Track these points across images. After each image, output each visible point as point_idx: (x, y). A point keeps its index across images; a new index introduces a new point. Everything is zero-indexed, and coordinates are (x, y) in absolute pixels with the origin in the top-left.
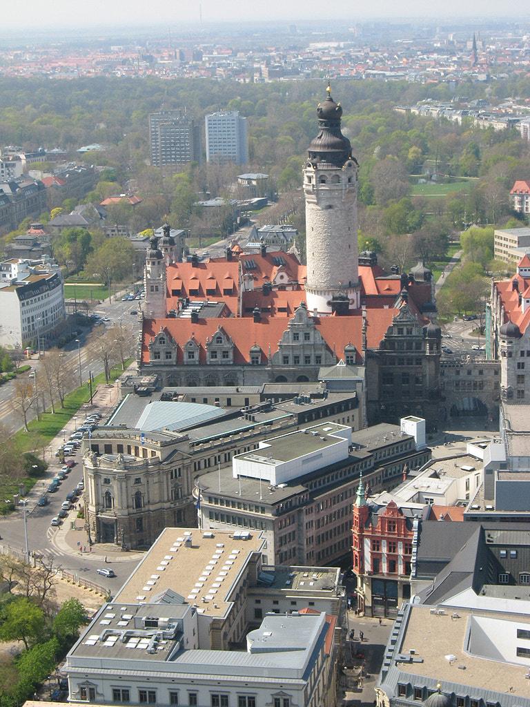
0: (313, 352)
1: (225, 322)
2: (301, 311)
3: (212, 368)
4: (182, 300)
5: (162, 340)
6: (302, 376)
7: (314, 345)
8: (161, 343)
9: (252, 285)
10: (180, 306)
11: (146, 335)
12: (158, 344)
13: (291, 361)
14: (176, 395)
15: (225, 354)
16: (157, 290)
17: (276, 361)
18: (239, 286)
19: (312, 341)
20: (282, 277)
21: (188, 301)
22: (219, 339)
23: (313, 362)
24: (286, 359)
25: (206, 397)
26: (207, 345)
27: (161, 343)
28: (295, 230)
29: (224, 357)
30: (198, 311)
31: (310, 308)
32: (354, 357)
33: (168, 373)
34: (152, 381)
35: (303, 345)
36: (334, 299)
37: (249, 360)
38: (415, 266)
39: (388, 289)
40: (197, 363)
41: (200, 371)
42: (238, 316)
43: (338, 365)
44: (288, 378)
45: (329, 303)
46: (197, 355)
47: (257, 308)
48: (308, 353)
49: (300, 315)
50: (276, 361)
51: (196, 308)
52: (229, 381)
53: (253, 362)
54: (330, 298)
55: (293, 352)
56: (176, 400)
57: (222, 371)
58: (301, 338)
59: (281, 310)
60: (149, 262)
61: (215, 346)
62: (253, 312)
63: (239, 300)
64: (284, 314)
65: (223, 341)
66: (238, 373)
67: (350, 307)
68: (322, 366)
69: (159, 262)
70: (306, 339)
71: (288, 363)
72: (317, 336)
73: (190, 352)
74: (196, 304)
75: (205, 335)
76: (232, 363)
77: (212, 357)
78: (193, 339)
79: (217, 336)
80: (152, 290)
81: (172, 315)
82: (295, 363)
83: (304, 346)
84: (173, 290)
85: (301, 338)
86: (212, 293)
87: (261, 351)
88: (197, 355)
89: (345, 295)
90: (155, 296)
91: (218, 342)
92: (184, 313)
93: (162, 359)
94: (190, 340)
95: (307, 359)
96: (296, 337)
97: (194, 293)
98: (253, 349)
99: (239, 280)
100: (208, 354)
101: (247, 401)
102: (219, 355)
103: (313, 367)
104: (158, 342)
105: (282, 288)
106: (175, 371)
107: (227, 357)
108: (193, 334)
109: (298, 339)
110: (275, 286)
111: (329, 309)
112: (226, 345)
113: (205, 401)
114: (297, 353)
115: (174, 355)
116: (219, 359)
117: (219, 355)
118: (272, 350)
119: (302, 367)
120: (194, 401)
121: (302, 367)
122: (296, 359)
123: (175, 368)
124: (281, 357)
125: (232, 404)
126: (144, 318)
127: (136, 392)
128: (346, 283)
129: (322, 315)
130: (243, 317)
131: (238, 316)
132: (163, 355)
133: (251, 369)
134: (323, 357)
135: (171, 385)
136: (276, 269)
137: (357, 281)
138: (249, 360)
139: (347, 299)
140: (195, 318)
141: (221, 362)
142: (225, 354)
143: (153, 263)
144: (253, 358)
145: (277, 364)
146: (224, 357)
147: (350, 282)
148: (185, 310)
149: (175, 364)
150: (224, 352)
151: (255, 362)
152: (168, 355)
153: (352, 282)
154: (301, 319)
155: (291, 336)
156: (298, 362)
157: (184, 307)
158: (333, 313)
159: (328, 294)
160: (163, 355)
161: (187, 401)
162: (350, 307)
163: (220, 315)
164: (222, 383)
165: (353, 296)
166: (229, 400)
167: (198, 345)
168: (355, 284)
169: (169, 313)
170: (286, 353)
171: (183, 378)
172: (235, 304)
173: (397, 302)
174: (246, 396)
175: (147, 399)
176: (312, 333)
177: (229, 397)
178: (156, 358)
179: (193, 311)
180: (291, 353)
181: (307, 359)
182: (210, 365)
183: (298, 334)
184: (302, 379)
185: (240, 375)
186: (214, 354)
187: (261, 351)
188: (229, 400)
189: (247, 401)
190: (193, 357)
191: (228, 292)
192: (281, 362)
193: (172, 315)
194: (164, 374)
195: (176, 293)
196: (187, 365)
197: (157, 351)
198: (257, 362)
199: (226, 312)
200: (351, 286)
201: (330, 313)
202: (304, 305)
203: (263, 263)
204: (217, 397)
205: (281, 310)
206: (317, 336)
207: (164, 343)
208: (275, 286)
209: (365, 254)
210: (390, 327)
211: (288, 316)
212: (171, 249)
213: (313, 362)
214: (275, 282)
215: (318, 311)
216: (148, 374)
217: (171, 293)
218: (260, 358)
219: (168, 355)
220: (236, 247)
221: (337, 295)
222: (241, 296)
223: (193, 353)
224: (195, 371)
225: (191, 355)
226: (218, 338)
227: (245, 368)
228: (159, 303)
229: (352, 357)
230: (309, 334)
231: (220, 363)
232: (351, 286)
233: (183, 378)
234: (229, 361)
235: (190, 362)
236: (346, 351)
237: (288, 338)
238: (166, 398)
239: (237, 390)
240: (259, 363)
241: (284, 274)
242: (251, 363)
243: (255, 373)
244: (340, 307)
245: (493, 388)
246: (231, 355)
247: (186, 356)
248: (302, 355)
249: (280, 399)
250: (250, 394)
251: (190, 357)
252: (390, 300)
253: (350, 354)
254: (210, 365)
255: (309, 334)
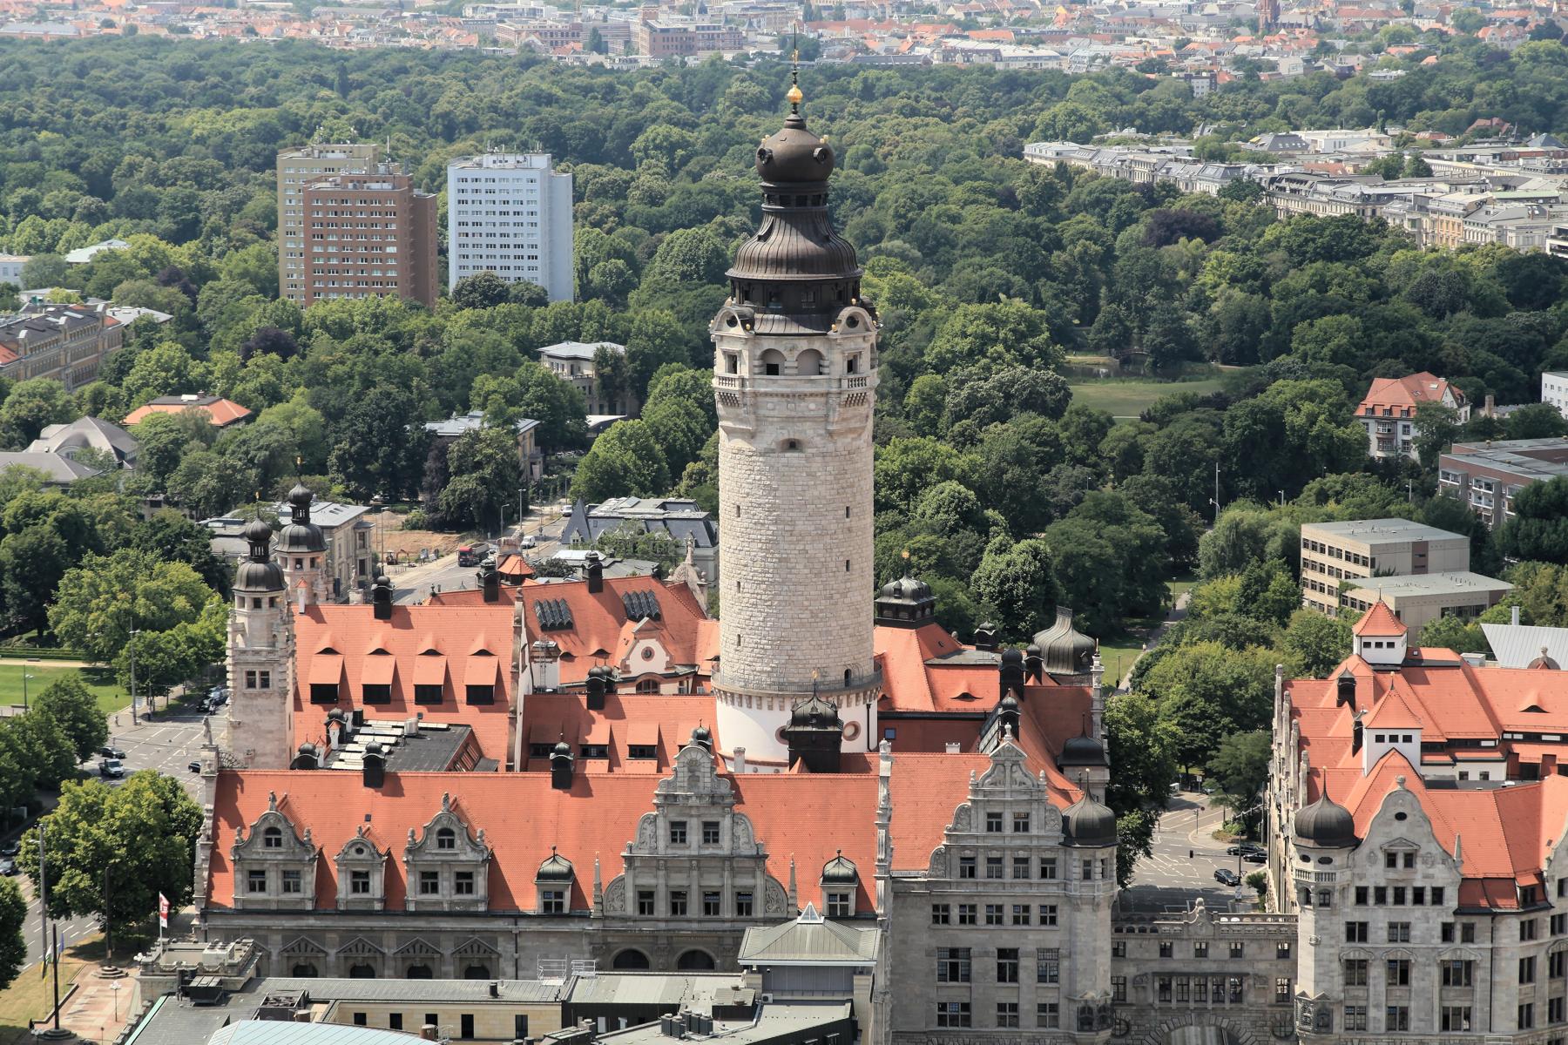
0: (727, 881)
1: (467, 787)
2: (694, 755)
3: (421, 924)
4: (340, 717)
5: (272, 836)
6: (694, 952)
7: (730, 858)
8: (268, 843)
9: (557, 675)
10: (335, 732)
11: (223, 824)
12: (259, 846)
13: (662, 907)
14: (307, 1001)
15: (464, 882)
16: (265, 684)
17: (617, 904)
18: (515, 676)
19: (725, 846)
20: (648, 654)
21: (359, 720)
22: (446, 837)
23: (728, 910)
24: (645, 900)
25: (397, 1009)
26: (409, 851)
27: (268, 843)
28: (702, 514)
29: (459, 889)
30: (385, 749)
31: (726, 747)
32: (853, 897)
33: (288, 934)
34: (237, 959)
35: (699, 858)
36: (797, 720)
37: (529, 902)
38: (1048, 623)
39: (966, 697)
40: (378, 906)
41: (383, 930)
42: (510, 768)
43: (799, 920)
44: (651, 959)
45: (783, 734)
46: (377, 882)
47: (562, 745)
48: (712, 881)
49: (693, 767)
50: (617, 904)
51: (380, 740)
52: (475, 964)
53: (547, 906)
54: (783, 718)
55: (667, 877)
56: (306, 1018)
57: (453, 931)
58: (694, 836)
59: (639, 752)
60: (242, 600)
61: (434, 854)
62: (552, 756)
63: (513, 721)
64: (648, 766)
65: (458, 842)
66: (500, 939)
67: (846, 747)
68: (756, 922)
69: (272, 602)
70: (706, 841)
71: (651, 912)
72: (739, 830)
73: (356, 875)
74: (383, 728)
75: (399, 822)
76: (482, 908)
77: (424, 889)
78: (365, 833)
79: (438, 828)
80: (251, 684)
81: (306, 761)
82: (674, 911)
83: (699, 862)
84: (313, 686)
85: (694, 836)
86: (430, 696)
87: (569, 875)
88: (377, 882)
89: (830, 711)
90: (260, 702)
91: (441, 844)
92: (342, 755)
93: (273, 893)
94: (355, 837)
95: (711, 905)
96: (678, 833)
97: (379, 696)
98: (549, 867)
99: (515, 658)
100: (409, 880)
101: (521, 1025)
102: (446, 884)
103: (727, 925)
104: (260, 841)
105: (648, 685)
106: (311, 931)
107: (470, 891)
108: (368, 818)
109: (683, 841)
110: (627, 681)
111: (782, 752)
112: (465, 855)
113: (396, 1022)
114: (679, 880)
115: (309, 880)
116: (446, 894)
117: (446, 884)
118: (601, 871)
119: (695, 926)
120: (360, 1020)
121: (695, 926)
122: (678, 902)
123: (312, 922)
124: (630, 894)
125: (478, 1031)
126: (221, 769)
127: (187, 992)
128: (837, 674)
129: (763, 770)
130: (524, 768)
131: (510, 768)
132: (273, 881)
133: (540, 928)
134: (759, 897)
135: (299, 972)
136: (631, 627)
137: (867, 669)
138: (529, 902)
139: (835, 720)
140: (376, 772)
141: (451, 903)
142: (464, 882)
143: (257, 604)
144: (545, 894)
145: (618, 913)
146: (459, 889)
147: (847, 673)
148: (350, 747)
149: (309, 907)
150: (459, 875)
151: (552, 910)
152: (291, 881)
153: (855, 673)
154: (694, 779)
155: (663, 831)
156: (684, 912)
157: (345, 738)
158: (791, 765)
159: (782, 708)
160: (273, 881)
161: (340, 1021)
162: (846, 747)
163: (454, 762)
164: (451, 969)
165: (854, 711)
166: (467, 1021)
167: (382, 850)
168: (861, 678)
169: (297, 754)
170: (647, 881)
171: (332, 952)
172: (499, 734)
173: (989, 736)
174: (520, 1010)
175: (217, 1014)
176: (726, 823)
177: (467, 1010)
178: (252, 889)
179: (369, 750)
180: (662, 881)
181: (711, 905)
182: (417, 915)
183: (683, 824)
184: (695, 961)
185: (504, 947)
186: (429, 882)
187: (569, 875)
188: (467, 1021)
189: (521, 1025)
190: (366, 888)
191: (482, 696)
192: (631, 909)
193: (306, 761)
194: (278, 938)
195: (324, 695)
196: (347, 913)
197: (256, 868)
198: (560, 906)
199: (468, 754)
200: (849, 683)
201: (784, 765)
202: (704, 740)
203: (587, 606)
204: (431, 1009)
205: (639, 752)
206: (739, 830)
207: (278, 843)
208: (627, 681)
209: (899, 592)
210: (962, 809)
211: (659, 770)
212: (313, 561)
213: (728, 910)
214: (626, 669)
215: (748, 755)
216: (229, 935)
217: (306, 694)
218: (568, 895)
219: (291, 881)
220: (513, 560)
221: (806, 709)
222: (520, 709)
223: (366, 875)
224: (372, 930)
225: (360, 881)
226: (441, 833)
227: (523, 925)
228: (270, 722)
229: (844, 897)
230: (716, 824)
231: (446, 908)
232: (849, 683)
233: (332, 952)
234: (476, 902)
235: (353, 901)
236: (828, 879)
237: (655, 836)
238: (275, 1012)
239: (494, 991)
240: (566, 910)
241: (653, 643)
242: (540, 911)
243: (552, 940)
244: (815, 746)
245: (1272, 998)
246: (481, 883)
247: (342, 884)
248: (695, 887)
249: (623, 1022)
250: (533, 1003)
251: (355, 889)
252: (962, 727)
253: (840, 888)
254: (417, 915)
255: (716, 824)
